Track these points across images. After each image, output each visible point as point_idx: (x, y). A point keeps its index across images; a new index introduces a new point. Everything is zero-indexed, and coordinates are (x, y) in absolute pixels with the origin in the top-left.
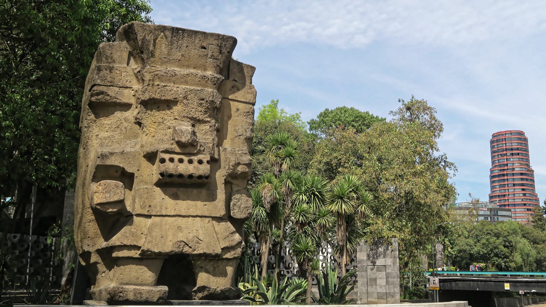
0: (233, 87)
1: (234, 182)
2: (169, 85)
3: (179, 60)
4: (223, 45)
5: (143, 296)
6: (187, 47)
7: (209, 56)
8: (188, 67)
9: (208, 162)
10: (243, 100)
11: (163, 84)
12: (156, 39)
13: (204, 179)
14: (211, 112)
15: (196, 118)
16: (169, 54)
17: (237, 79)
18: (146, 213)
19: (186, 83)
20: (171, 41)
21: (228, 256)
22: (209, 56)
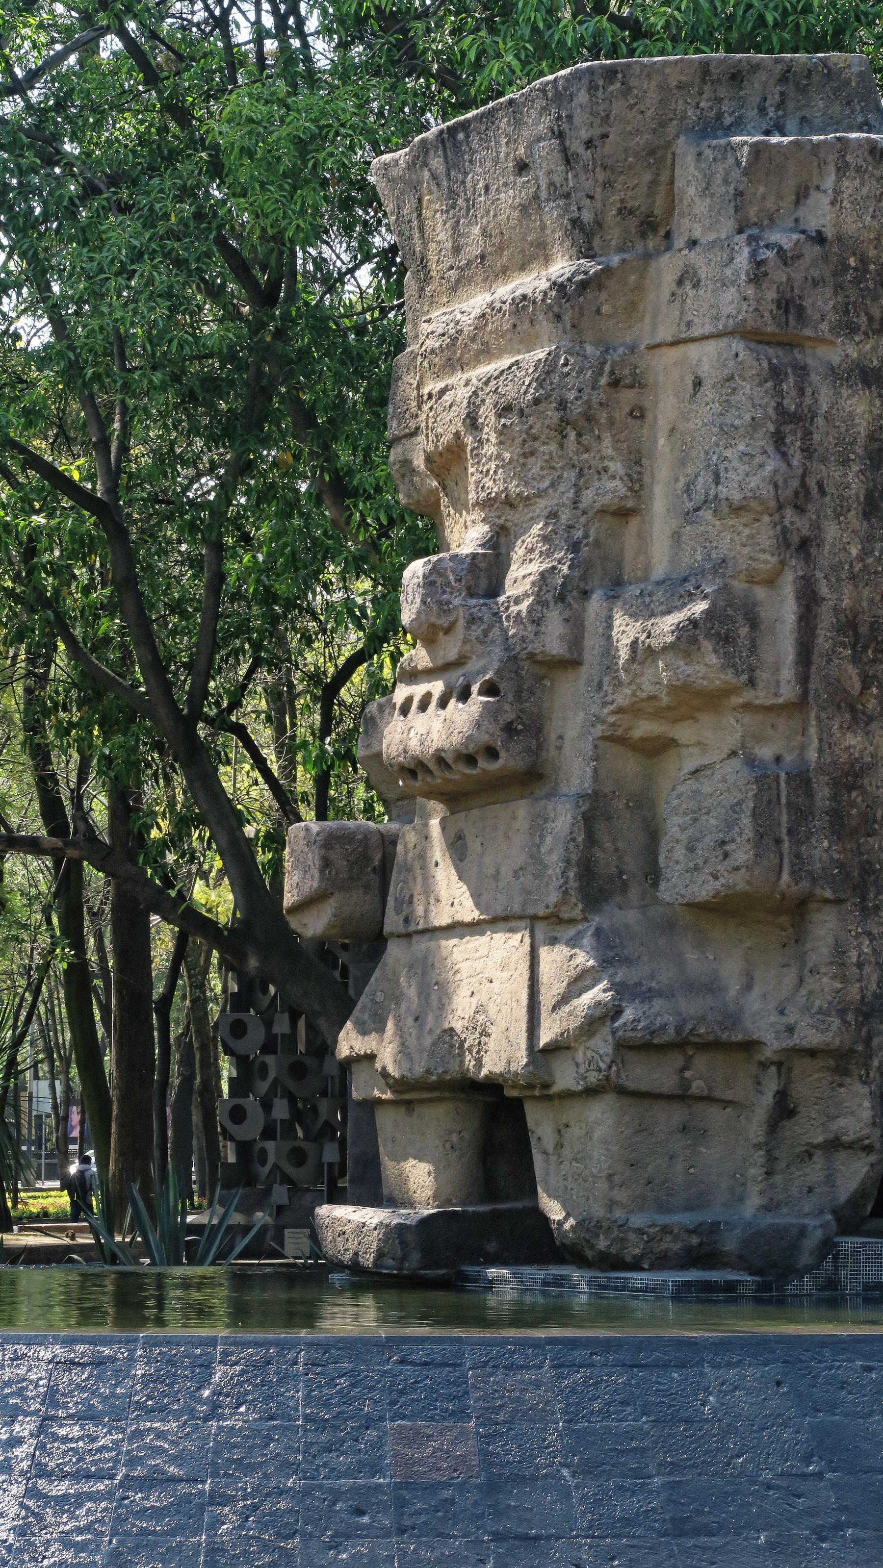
0: (680, 282)
1: (683, 733)
2: (451, 381)
3: (483, 257)
4: (565, 127)
5: (349, 1245)
6: (487, 188)
7: (544, 194)
8: (505, 273)
9: (490, 689)
10: (707, 329)
11: (441, 385)
12: (420, 201)
13: (483, 763)
14: (553, 447)
15: (495, 499)
16: (457, 250)
17: (697, 234)
18: (401, 929)
19: (486, 353)
20: (450, 190)
21: (566, 1077)
22: (544, 194)
